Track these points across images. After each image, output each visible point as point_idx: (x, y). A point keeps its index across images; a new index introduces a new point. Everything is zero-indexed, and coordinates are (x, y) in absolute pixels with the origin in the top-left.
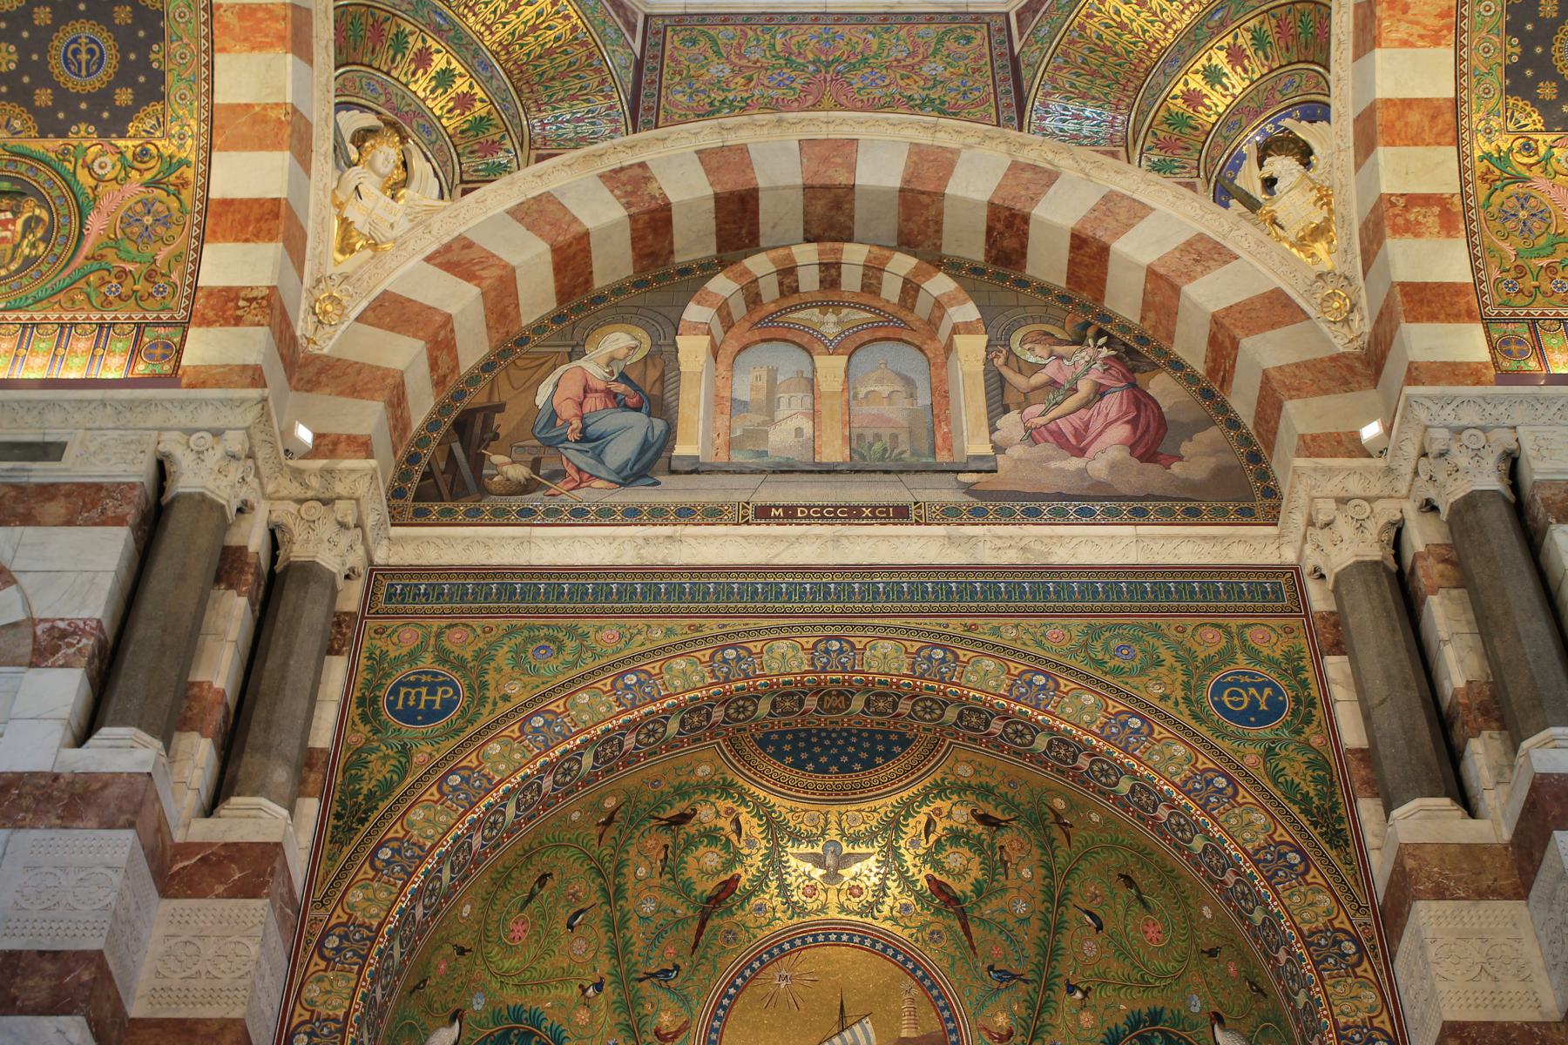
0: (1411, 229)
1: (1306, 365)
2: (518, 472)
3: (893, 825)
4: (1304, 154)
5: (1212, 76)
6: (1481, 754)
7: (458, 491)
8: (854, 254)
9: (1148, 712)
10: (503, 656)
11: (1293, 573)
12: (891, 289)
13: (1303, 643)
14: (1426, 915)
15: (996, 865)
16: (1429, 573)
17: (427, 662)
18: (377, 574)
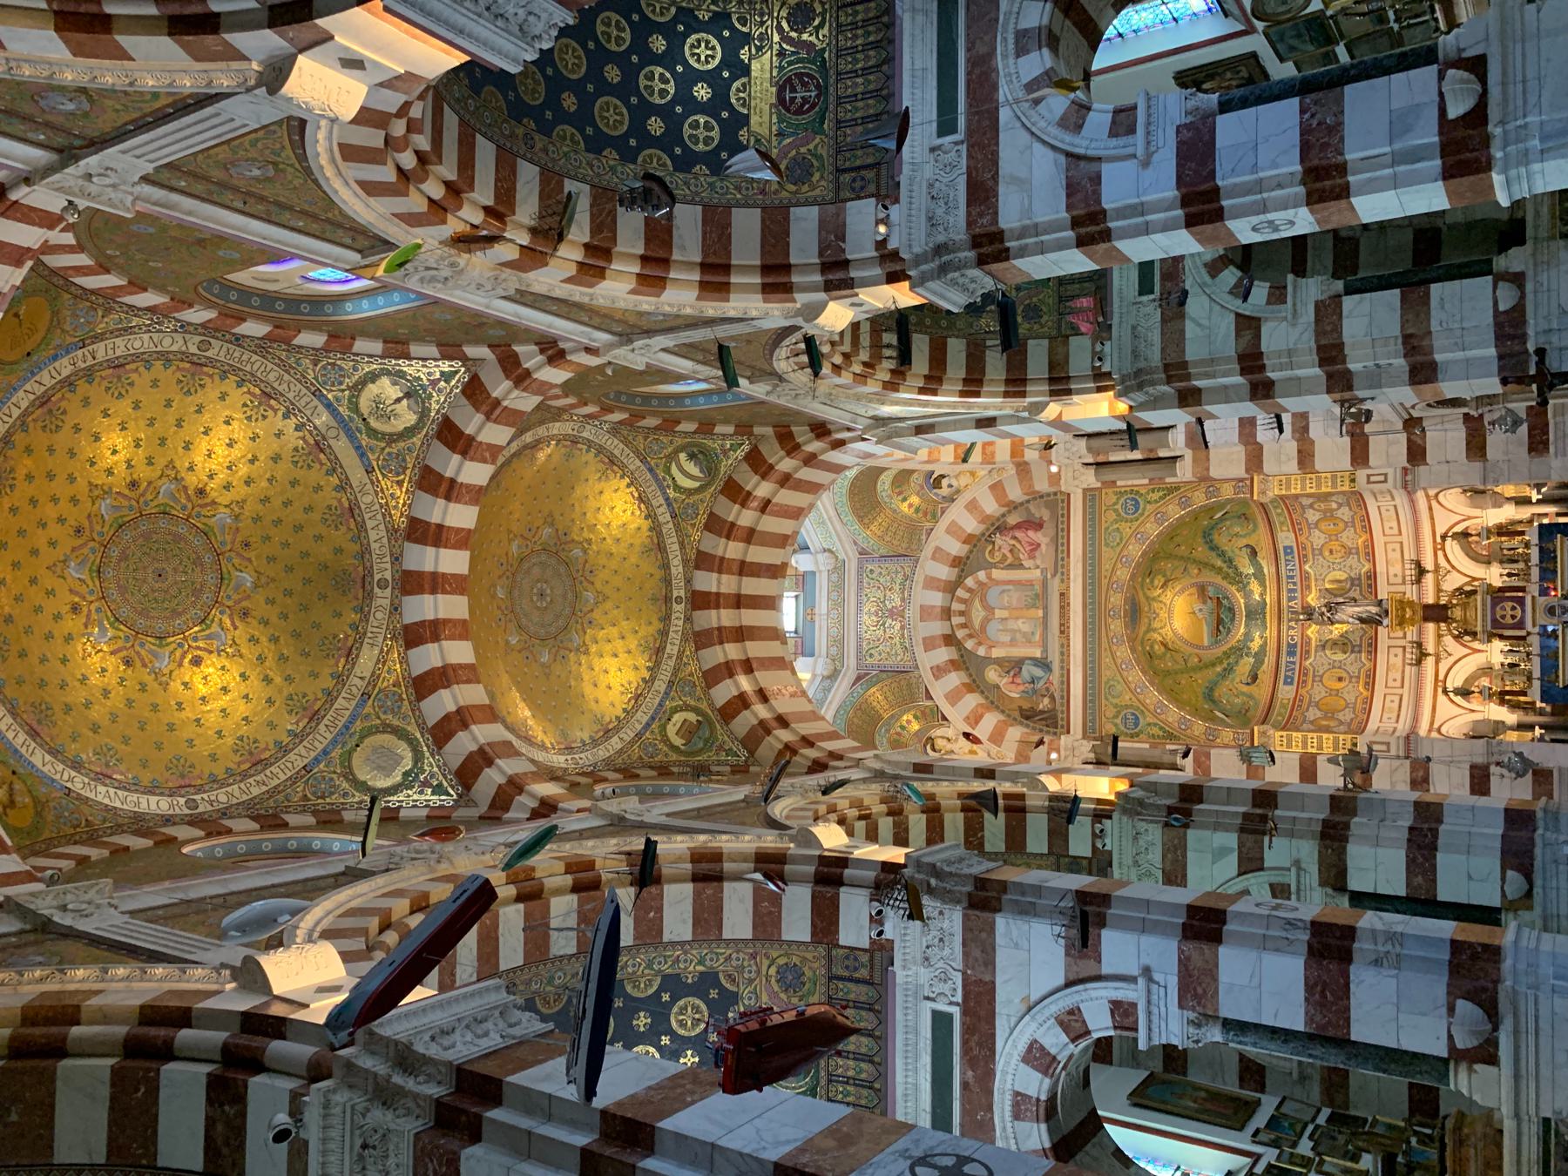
0: (993, 454)
1: (1021, 482)
2: (1046, 700)
3: (1147, 598)
4: (943, 476)
5: (905, 499)
6: (1162, 453)
7: (1055, 717)
8: (956, 606)
9: (1135, 533)
10: (1115, 701)
11: (1085, 490)
12: (966, 595)
13: (1110, 491)
14: (1213, 473)
15: (1159, 572)
16: (1101, 459)
17: (1118, 721)
18: (1084, 737)
